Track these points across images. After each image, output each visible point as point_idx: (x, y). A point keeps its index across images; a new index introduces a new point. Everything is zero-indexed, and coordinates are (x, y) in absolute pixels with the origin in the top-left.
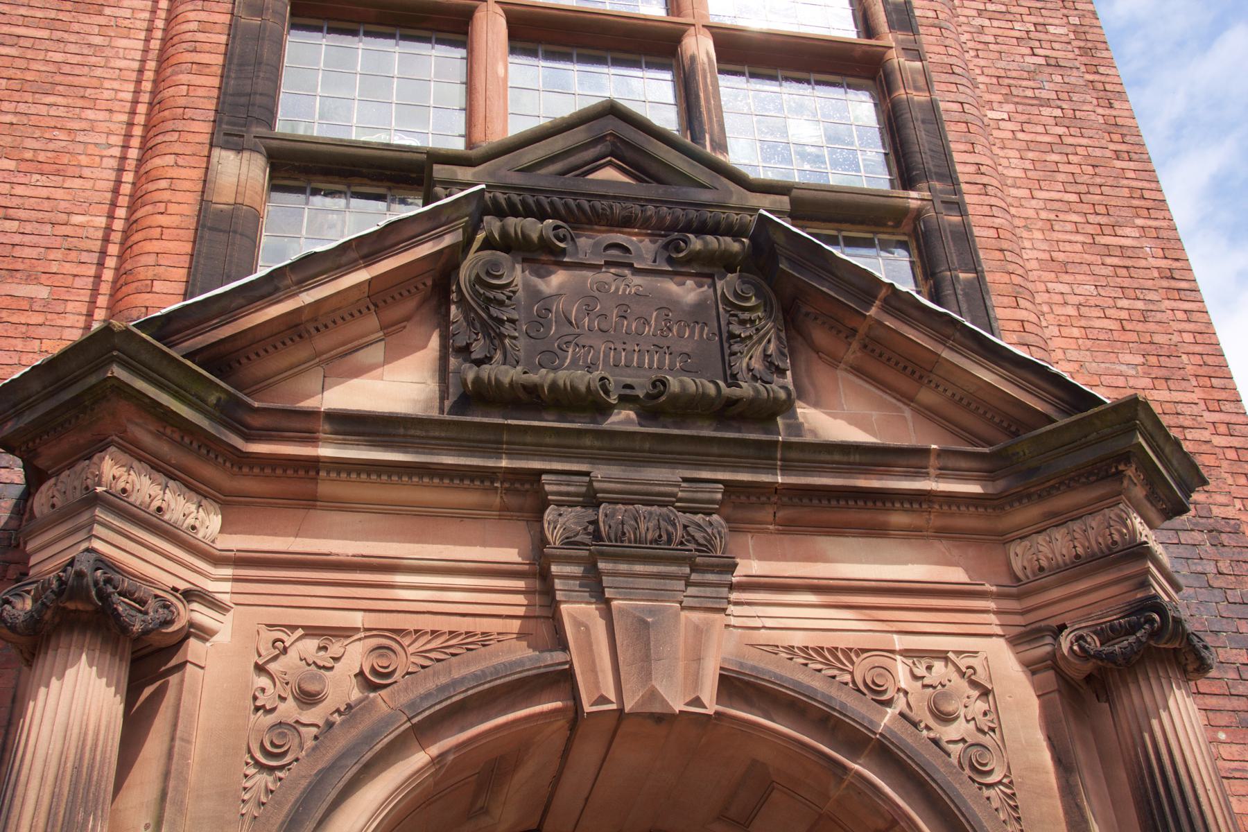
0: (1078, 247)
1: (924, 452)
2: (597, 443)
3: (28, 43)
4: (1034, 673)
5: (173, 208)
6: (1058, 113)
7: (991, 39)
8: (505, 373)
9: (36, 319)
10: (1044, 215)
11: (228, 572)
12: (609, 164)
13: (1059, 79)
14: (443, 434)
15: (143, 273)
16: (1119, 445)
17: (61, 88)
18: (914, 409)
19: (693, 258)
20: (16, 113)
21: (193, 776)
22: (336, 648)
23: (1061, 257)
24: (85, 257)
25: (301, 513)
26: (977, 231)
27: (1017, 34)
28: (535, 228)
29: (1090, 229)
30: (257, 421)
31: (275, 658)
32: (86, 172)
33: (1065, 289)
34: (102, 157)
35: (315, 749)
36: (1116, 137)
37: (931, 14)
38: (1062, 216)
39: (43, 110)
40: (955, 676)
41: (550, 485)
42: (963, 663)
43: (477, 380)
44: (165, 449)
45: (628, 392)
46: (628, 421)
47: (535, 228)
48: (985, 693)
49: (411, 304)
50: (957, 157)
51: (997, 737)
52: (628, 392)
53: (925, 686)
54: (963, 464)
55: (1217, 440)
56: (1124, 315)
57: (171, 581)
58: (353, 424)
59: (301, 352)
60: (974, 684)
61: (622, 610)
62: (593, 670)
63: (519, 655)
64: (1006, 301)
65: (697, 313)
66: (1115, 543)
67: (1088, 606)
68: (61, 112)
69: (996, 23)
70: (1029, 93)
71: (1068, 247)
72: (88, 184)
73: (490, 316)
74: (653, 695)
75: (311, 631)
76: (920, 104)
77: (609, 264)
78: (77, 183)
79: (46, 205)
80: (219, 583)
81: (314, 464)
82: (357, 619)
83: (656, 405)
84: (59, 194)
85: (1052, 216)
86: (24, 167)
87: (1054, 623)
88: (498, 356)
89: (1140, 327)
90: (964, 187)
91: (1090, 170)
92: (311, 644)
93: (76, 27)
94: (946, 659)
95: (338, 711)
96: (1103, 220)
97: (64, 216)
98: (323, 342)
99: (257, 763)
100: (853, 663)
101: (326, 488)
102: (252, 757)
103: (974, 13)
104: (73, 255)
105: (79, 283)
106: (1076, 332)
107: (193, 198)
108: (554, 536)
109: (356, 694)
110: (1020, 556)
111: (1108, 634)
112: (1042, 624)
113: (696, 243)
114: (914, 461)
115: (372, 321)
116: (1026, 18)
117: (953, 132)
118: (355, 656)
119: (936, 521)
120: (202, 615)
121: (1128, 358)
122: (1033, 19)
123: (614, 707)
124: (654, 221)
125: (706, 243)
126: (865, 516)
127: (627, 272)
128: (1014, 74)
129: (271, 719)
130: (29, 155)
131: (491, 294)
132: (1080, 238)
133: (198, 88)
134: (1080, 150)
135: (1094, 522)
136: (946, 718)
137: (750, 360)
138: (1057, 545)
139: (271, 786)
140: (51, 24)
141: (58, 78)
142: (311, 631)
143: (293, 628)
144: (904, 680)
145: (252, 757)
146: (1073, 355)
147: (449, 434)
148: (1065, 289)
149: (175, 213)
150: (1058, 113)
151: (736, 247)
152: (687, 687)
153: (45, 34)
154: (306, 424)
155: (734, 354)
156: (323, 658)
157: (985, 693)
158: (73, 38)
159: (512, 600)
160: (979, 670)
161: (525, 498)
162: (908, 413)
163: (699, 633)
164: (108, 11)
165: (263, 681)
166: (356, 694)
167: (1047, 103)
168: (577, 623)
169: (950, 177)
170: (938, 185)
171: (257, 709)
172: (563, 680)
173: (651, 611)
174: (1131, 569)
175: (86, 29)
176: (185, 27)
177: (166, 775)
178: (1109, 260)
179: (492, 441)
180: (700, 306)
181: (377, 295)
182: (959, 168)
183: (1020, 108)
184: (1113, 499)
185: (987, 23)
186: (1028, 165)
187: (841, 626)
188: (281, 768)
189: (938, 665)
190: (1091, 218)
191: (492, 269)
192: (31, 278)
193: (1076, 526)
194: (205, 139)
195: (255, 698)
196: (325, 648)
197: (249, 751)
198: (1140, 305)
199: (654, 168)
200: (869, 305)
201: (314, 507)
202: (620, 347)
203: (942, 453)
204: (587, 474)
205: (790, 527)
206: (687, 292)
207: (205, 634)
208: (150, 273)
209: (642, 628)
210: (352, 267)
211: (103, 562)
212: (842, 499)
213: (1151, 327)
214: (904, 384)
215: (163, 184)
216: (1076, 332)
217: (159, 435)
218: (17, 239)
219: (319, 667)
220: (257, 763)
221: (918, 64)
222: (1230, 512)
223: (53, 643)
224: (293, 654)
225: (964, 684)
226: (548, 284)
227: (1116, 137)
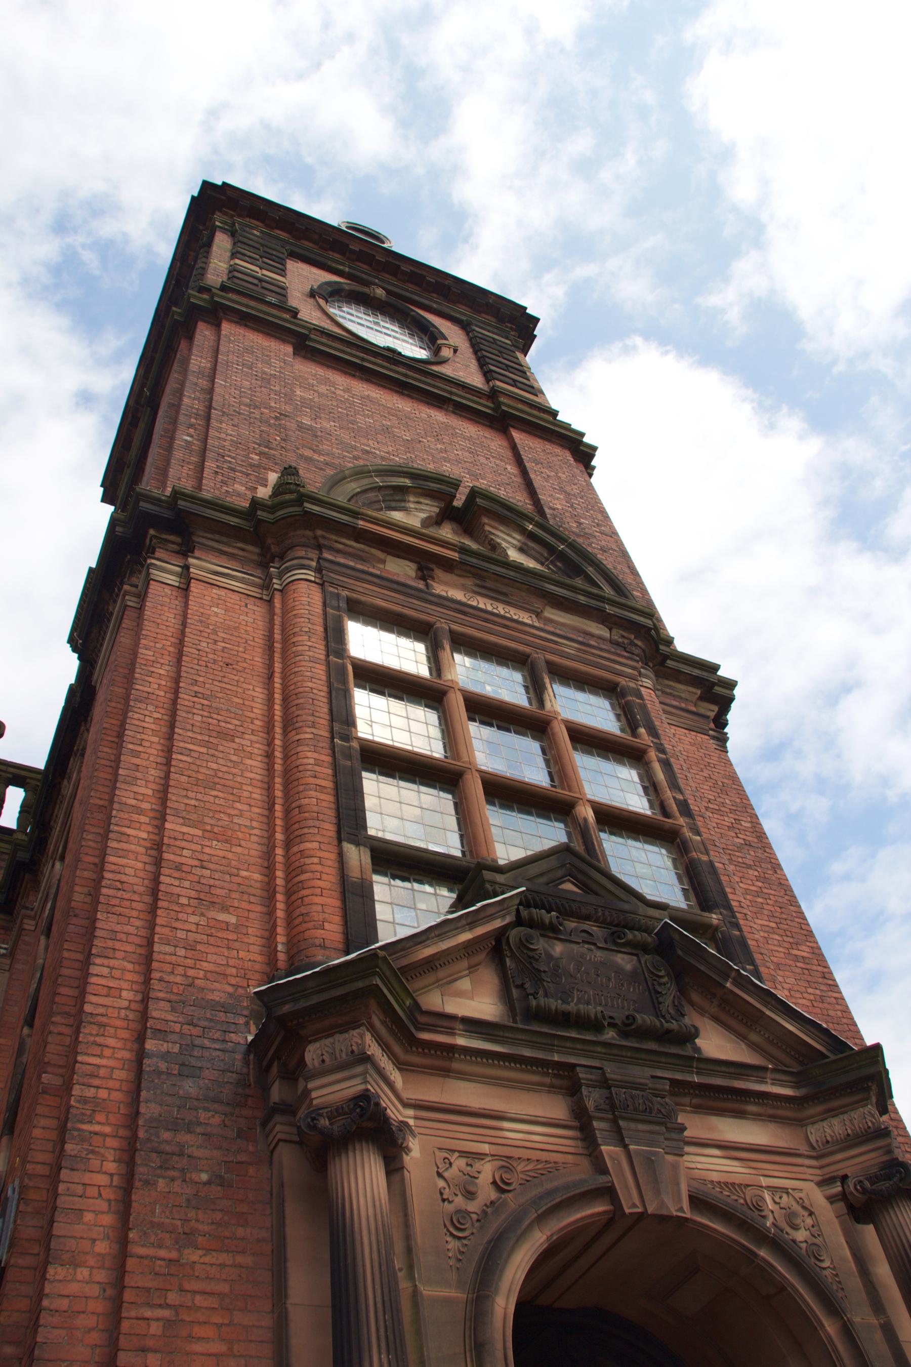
0: (782, 955)
2: (603, 1050)
3: (196, 755)
4: (831, 1203)
5: (324, 877)
6: (756, 873)
9: (233, 936)
12: (569, 880)
13: (752, 853)
14: (523, 1038)
17: (218, 786)
18: (746, 1044)
19: (628, 944)
20: (197, 800)
21: (419, 1241)
22: (478, 1165)
25: (441, 1079)
28: (549, 917)
29: (786, 945)
31: (447, 1169)
32: (243, 843)
34: (250, 835)
35: (481, 1227)
38: (771, 936)
39: (212, 799)
41: (582, 1074)
42: (797, 1195)
43: (538, 1006)
45: (612, 1021)
46: (613, 1038)
47: (549, 917)
48: (811, 1214)
49: (482, 956)
51: (821, 1239)
52: (612, 1021)
53: (781, 1208)
54: (784, 1077)
59: (431, 978)
60: (804, 1208)
61: (636, 1151)
66: (869, 1127)
68: (222, 802)
71: (777, 954)
72: (246, 852)
73: (534, 968)
74: (662, 1204)
75: (464, 1154)
76: (704, 861)
77: (583, 942)
78: (239, 850)
79: (224, 862)
81: (452, 1049)
82: (486, 1148)
83: (628, 1028)
84: (230, 855)
85: (766, 935)
86: (207, 834)
87: (841, 1173)
88: (541, 992)
89: (821, 1005)
91: (778, 909)
93: (221, 748)
94: (788, 1193)
95: (486, 1205)
97: (236, 871)
98: (442, 973)
99: (452, 1234)
100: (744, 1193)
101: (456, 1065)
102: (448, 1230)
104: (245, 897)
108: (590, 1104)
110: (815, 1133)
112: (835, 1174)
113: (630, 935)
114: (761, 1074)
115: (465, 964)
118: (487, 1171)
123: (640, 1210)
124: (601, 919)
125: (635, 936)
126: (736, 1106)
127: (593, 947)
128: (730, 847)
130: (208, 828)
131: (531, 954)
132: (781, 949)
136: (795, 1228)
138: (835, 1127)
139: (461, 1249)
140: (207, 744)
141: (216, 780)
142: (464, 1154)
143: (453, 1151)
144: (771, 1205)
145: (448, 1230)
147: (528, 1038)
150: (756, 873)
151: (649, 939)
153: (204, 750)
155: (661, 1003)
157: (811, 1214)
158: (221, 755)
160: (806, 1200)
162: (744, 1046)
164: (237, 740)
166: (493, 1195)
167: (749, 867)
168: (613, 1159)
169: (729, 907)
170: (725, 912)
171: (444, 1200)
172: (609, 1192)
175: (227, 750)
176: (306, 761)
180: (634, 973)
181: (469, 948)
183: (738, 868)
188: (465, 1238)
191: (529, 939)
192: (225, 909)
195: (441, 1194)
196: (471, 1165)
197: (445, 1226)
199: (594, 886)
200: (727, 980)
201: (448, 1076)
202: (600, 993)
204: (601, 1069)
206: (625, 961)
208: (321, 917)
209: (650, 1162)
210: (463, 929)
212: (724, 1094)
214: (742, 1029)
217: (383, 1023)
218: (212, 882)
219: (471, 1177)
220: (452, 1234)
221: (698, 838)
223: (350, 1147)
224: (454, 1167)
226: (554, 950)
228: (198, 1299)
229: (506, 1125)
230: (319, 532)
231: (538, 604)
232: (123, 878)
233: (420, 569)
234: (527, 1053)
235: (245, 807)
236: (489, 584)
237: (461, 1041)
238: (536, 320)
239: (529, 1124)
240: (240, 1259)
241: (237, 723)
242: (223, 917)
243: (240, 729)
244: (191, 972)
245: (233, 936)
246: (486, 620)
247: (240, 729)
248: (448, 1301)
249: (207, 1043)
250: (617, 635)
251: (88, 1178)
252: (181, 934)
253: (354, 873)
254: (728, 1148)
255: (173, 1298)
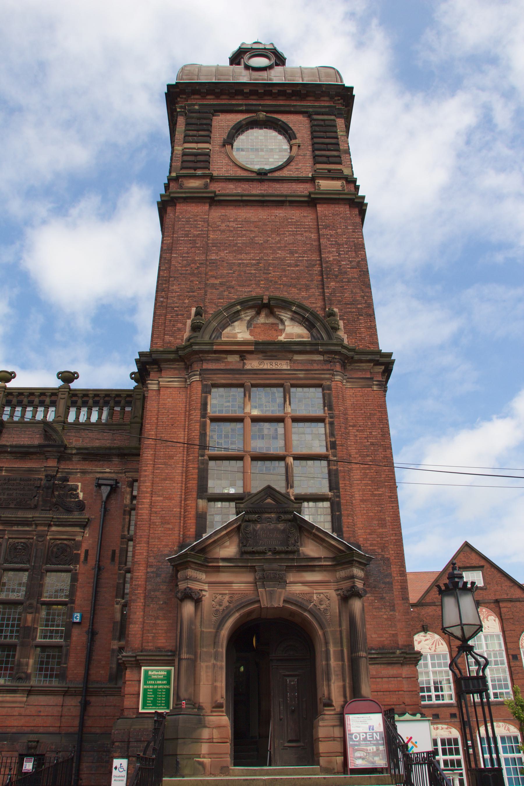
1: (321, 558)
5: (192, 513)
6: (371, 458)
7: (358, 438)
8: (250, 549)
10: (363, 487)
11: (207, 585)
13: (372, 448)
15: (188, 527)
16: (351, 559)
21: (205, 618)
23: (364, 498)
24: (177, 518)
26: (342, 501)
27: (365, 436)
30: (210, 560)
33: (364, 506)
36: (385, 460)
37: (340, 442)
40: (324, 597)
41: (257, 568)
44: (196, 567)
46: (270, 555)
50: (340, 482)
55: (392, 538)
56: (376, 511)
57: (199, 588)
58: (224, 560)
59: (216, 545)
62: (263, 600)
63: (252, 597)
64: (346, 518)
65: (283, 531)
67: (346, 585)
69: (360, 433)
70: (365, 453)
71: (367, 495)
74: (272, 605)
75: (220, 594)
78: (173, 501)
80: (206, 587)
81: (219, 566)
82: (227, 592)
84: (171, 504)
89: (379, 514)
90: (341, 490)
92: (220, 596)
96: (376, 487)
98: (219, 543)
101: (221, 570)
103: (356, 431)
105: (176, 524)
106: (365, 517)
107: (194, 510)
109: (228, 604)
111: (348, 591)
115: (227, 538)
116: (368, 431)
117: (341, 475)
118: (227, 598)
119: (324, 569)
120: (204, 593)
121: (376, 522)
122: (369, 431)
129: (215, 609)
133: (193, 484)
134: (374, 469)
135: (348, 570)
136: (321, 605)
137: (292, 541)
142: (220, 594)
146: (363, 522)
148: (364, 506)
149: (192, 513)
150: (371, 458)
152: (278, 603)
154: (217, 560)
156: (222, 598)
159: (251, 587)
161: (253, 569)
162: (321, 547)
163: (280, 593)
165: (213, 603)
166: (228, 604)
168: (261, 593)
170: (335, 491)
173: (272, 590)
174: (352, 580)
177: (201, 618)
178: (375, 498)
179: (247, 560)
181: (227, 534)
182: (340, 485)
184: (352, 566)
185: (358, 433)
186: (362, 474)
187: (306, 589)
189: (322, 595)
190: (373, 487)
192: (169, 524)
193: (346, 571)
194: (195, 496)
198: (380, 509)
203: (324, 558)
205: (298, 571)
206: (281, 526)
207: (204, 596)
210: (223, 531)
211: (190, 589)
213: (381, 514)
214: (320, 542)
215: (190, 507)
216: (365, 517)
218: (165, 515)
222: (388, 556)
225: (325, 598)
227: (385, 460)
228: (160, 631)
229: (233, 585)
230: (201, 355)
231: (290, 356)
232: (143, 517)
233: (241, 357)
234: (240, 565)
235: (176, 485)
236: (269, 354)
237: (221, 564)
238: (351, 89)
239: (240, 583)
240: (169, 621)
241: (174, 450)
242: (168, 526)
243: (176, 453)
244: (159, 546)
245: (171, 532)
246: (266, 374)
247: (176, 453)
248: (210, 632)
249: (163, 566)
250: (326, 357)
251: (137, 604)
252: (156, 535)
253: (200, 510)
254: (304, 583)
255: (154, 631)
